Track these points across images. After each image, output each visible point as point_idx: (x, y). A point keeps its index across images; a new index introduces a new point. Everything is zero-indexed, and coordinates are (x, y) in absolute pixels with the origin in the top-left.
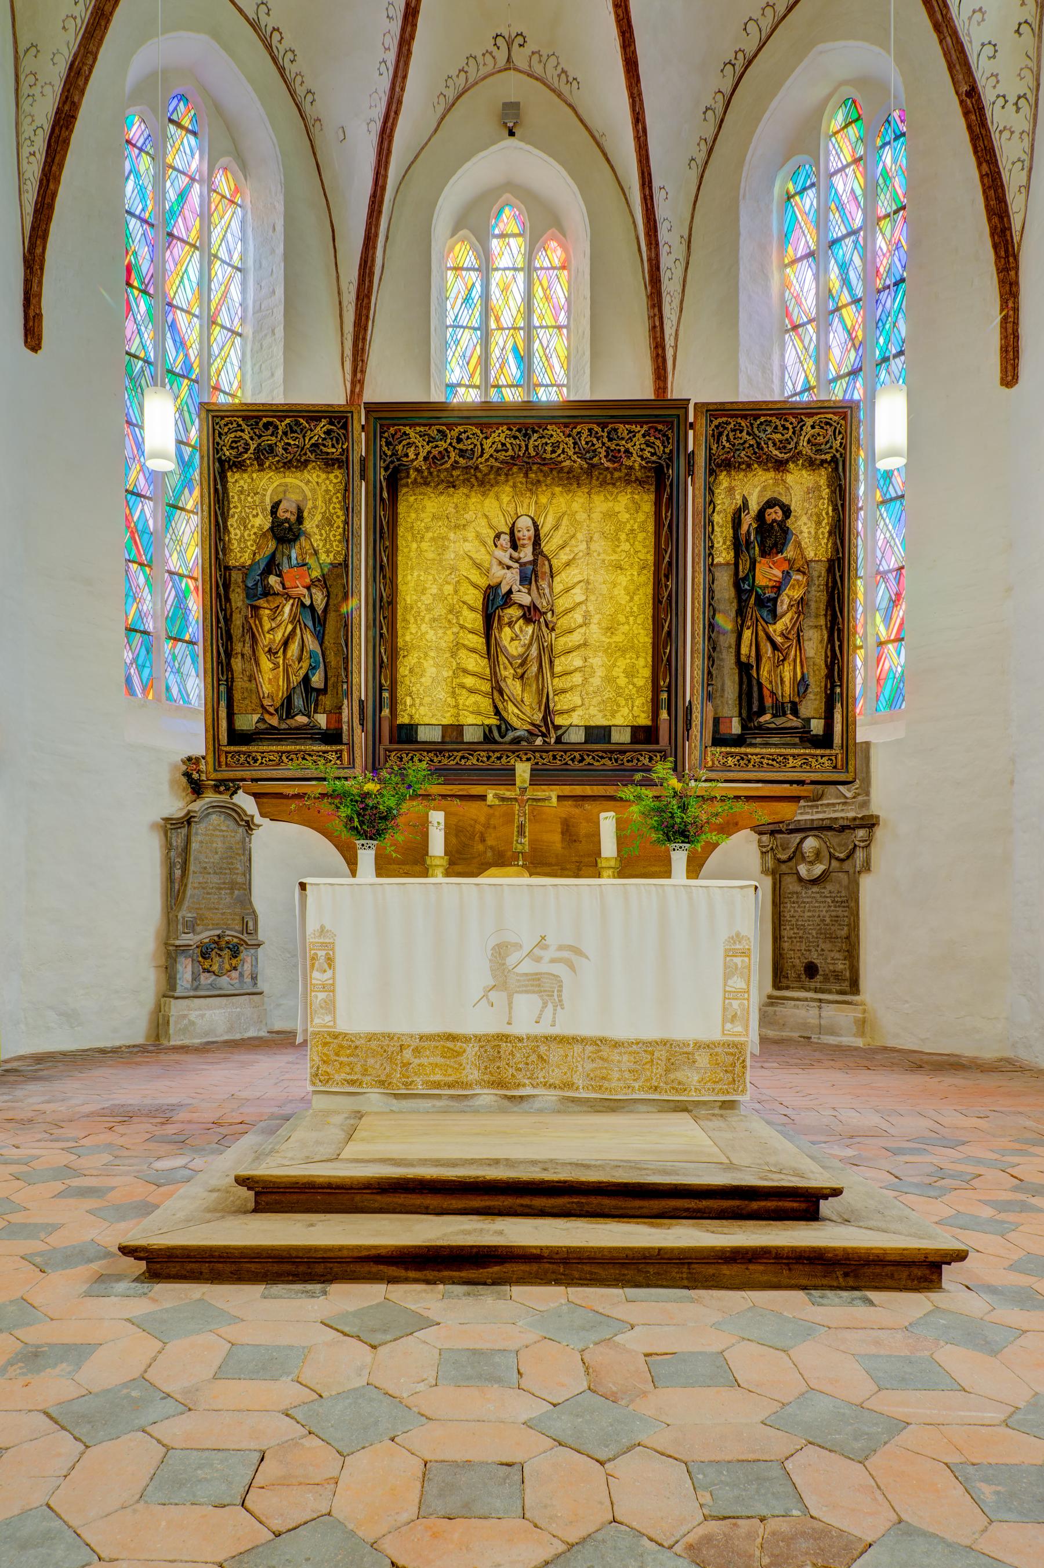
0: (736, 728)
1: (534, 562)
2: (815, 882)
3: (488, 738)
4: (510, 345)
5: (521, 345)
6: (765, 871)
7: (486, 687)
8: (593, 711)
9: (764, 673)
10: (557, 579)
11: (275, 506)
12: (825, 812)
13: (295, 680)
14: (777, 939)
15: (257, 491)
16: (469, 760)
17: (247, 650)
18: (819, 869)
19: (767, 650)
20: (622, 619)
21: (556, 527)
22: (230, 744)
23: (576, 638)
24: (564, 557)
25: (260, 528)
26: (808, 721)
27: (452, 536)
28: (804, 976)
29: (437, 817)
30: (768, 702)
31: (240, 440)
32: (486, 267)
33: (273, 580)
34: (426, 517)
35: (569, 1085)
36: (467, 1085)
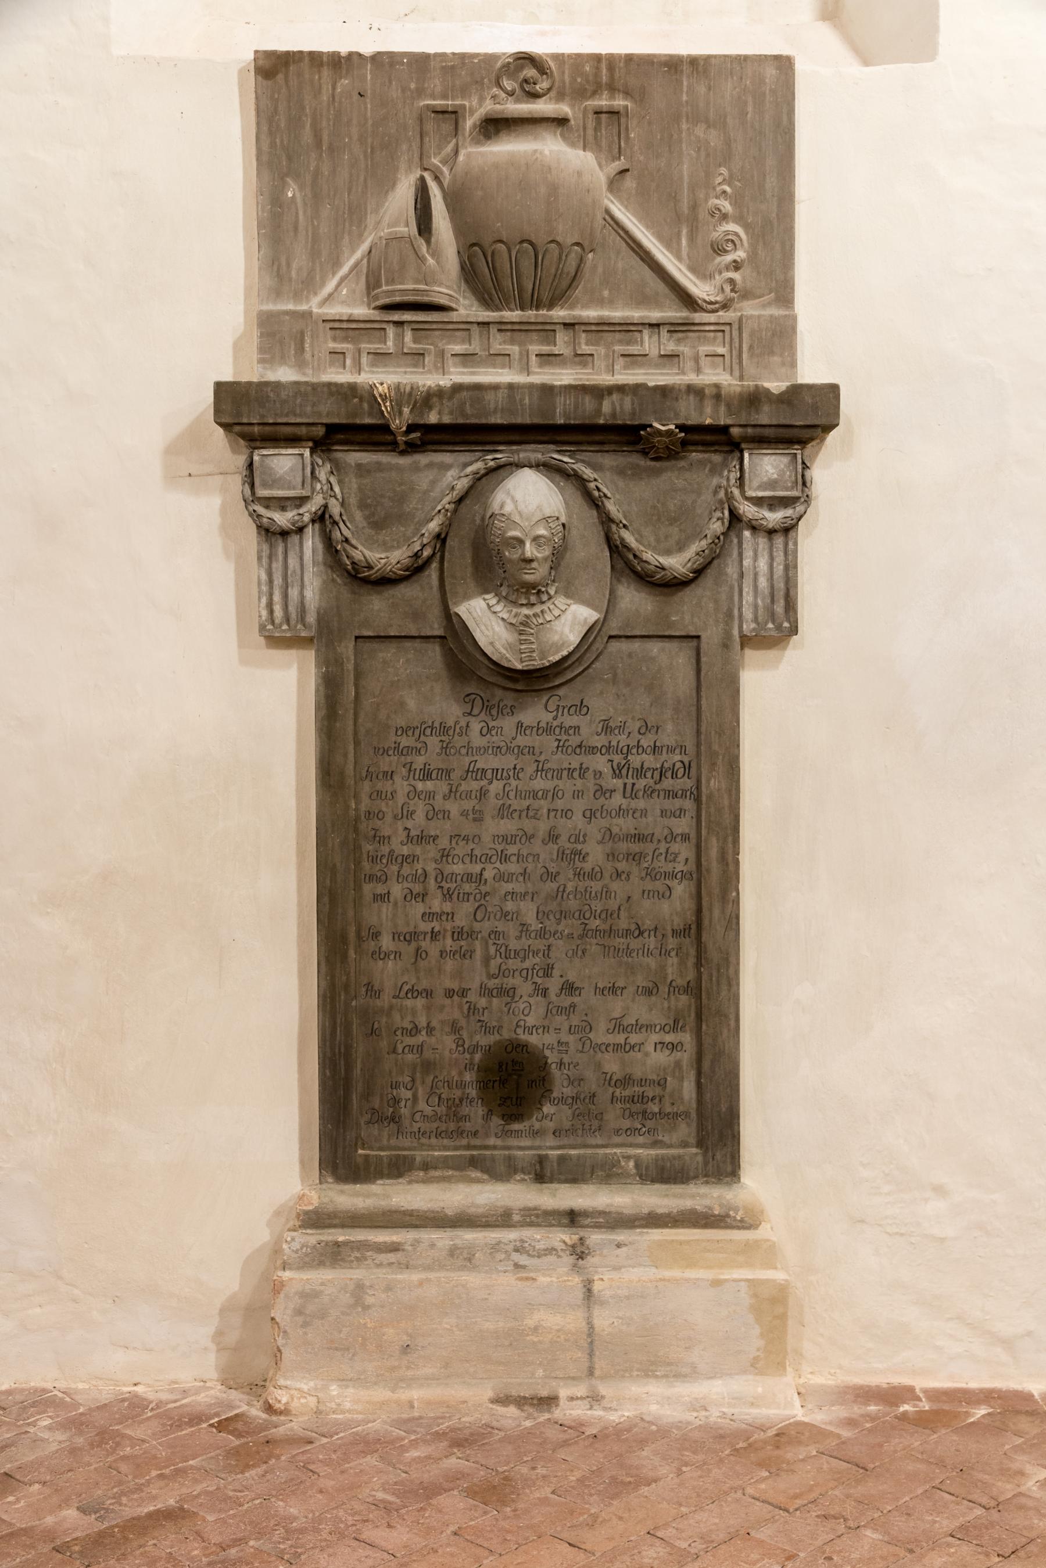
12: (582, 359)
28: (478, 1111)
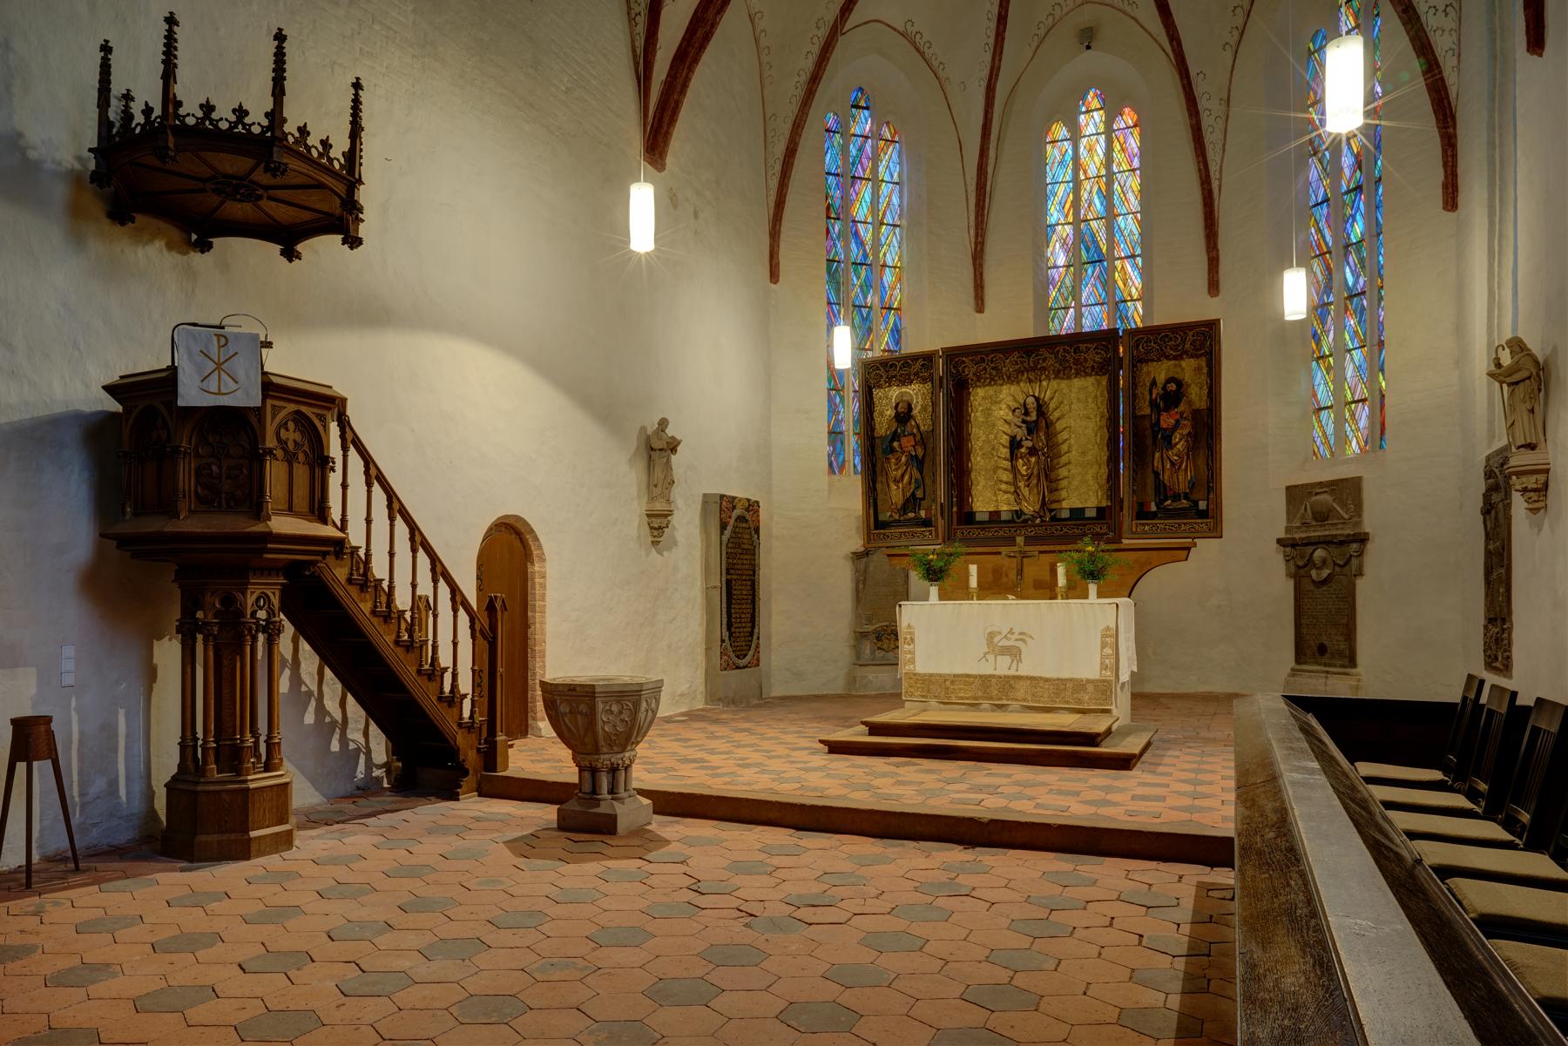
2: (1324, 582)
4: (1095, 189)
5: (1104, 188)
6: (1289, 575)
18: (1325, 573)
32: (1075, 136)
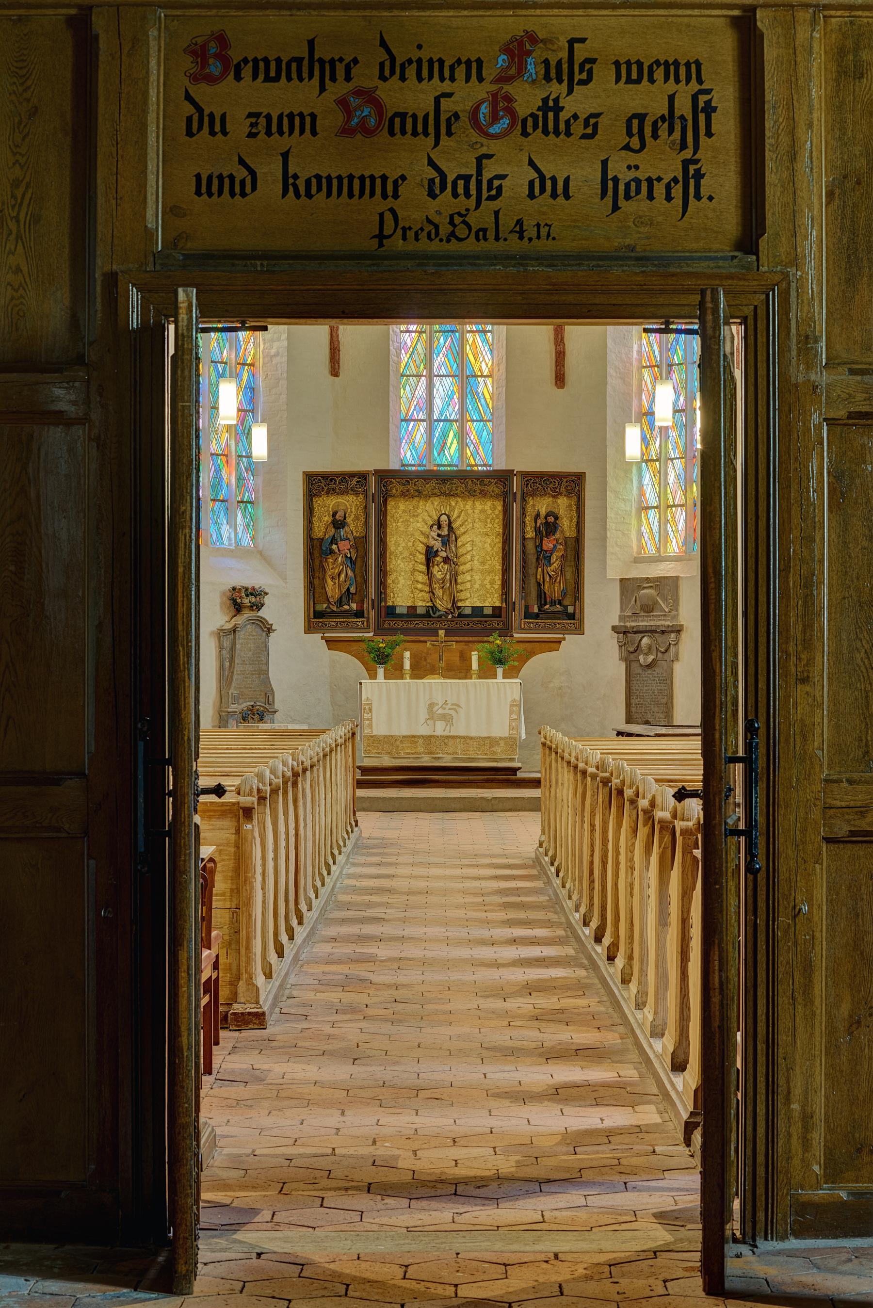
0: (536, 610)
1: (448, 535)
2: (649, 666)
3: (428, 612)
6: (621, 659)
7: (427, 589)
8: (475, 600)
9: (546, 588)
10: (459, 540)
11: (335, 514)
13: (344, 590)
14: (628, 705)
15: (327, 504)
16: (420, 622)
17: (321, 575)
18: (651, 658)
19: (548, 578)
20: (488, 558)
21: (459, 517)
22: (315, 618)
23: (468, 566)
24: (462, 530)
25: (327, 521)
26: (566, 607)
27: (411, 520)
29: (407, 654)
30: (548, 600)
31: (318, 484)
33: (334, 547)
34: (400, 511)
35: (456, 753)
36: (420, 754)
